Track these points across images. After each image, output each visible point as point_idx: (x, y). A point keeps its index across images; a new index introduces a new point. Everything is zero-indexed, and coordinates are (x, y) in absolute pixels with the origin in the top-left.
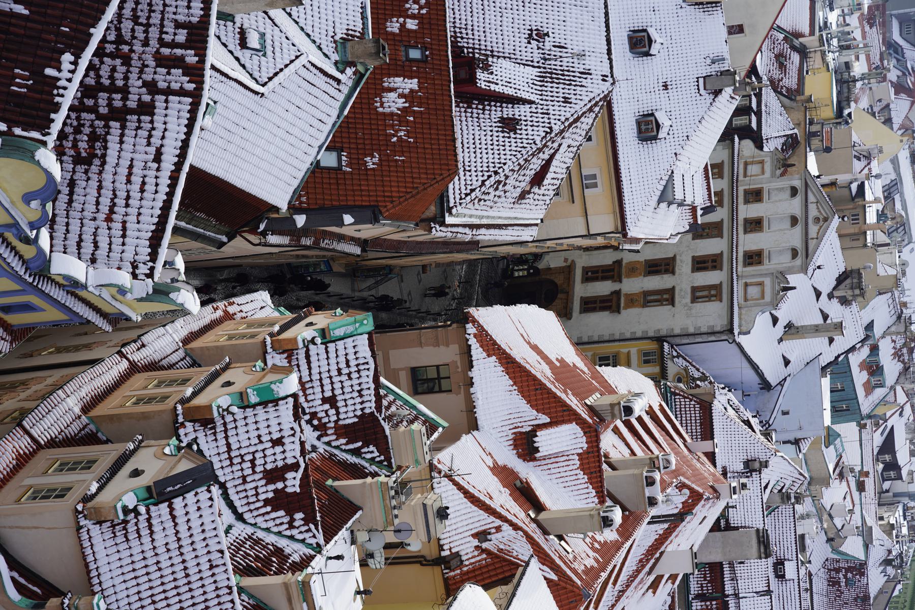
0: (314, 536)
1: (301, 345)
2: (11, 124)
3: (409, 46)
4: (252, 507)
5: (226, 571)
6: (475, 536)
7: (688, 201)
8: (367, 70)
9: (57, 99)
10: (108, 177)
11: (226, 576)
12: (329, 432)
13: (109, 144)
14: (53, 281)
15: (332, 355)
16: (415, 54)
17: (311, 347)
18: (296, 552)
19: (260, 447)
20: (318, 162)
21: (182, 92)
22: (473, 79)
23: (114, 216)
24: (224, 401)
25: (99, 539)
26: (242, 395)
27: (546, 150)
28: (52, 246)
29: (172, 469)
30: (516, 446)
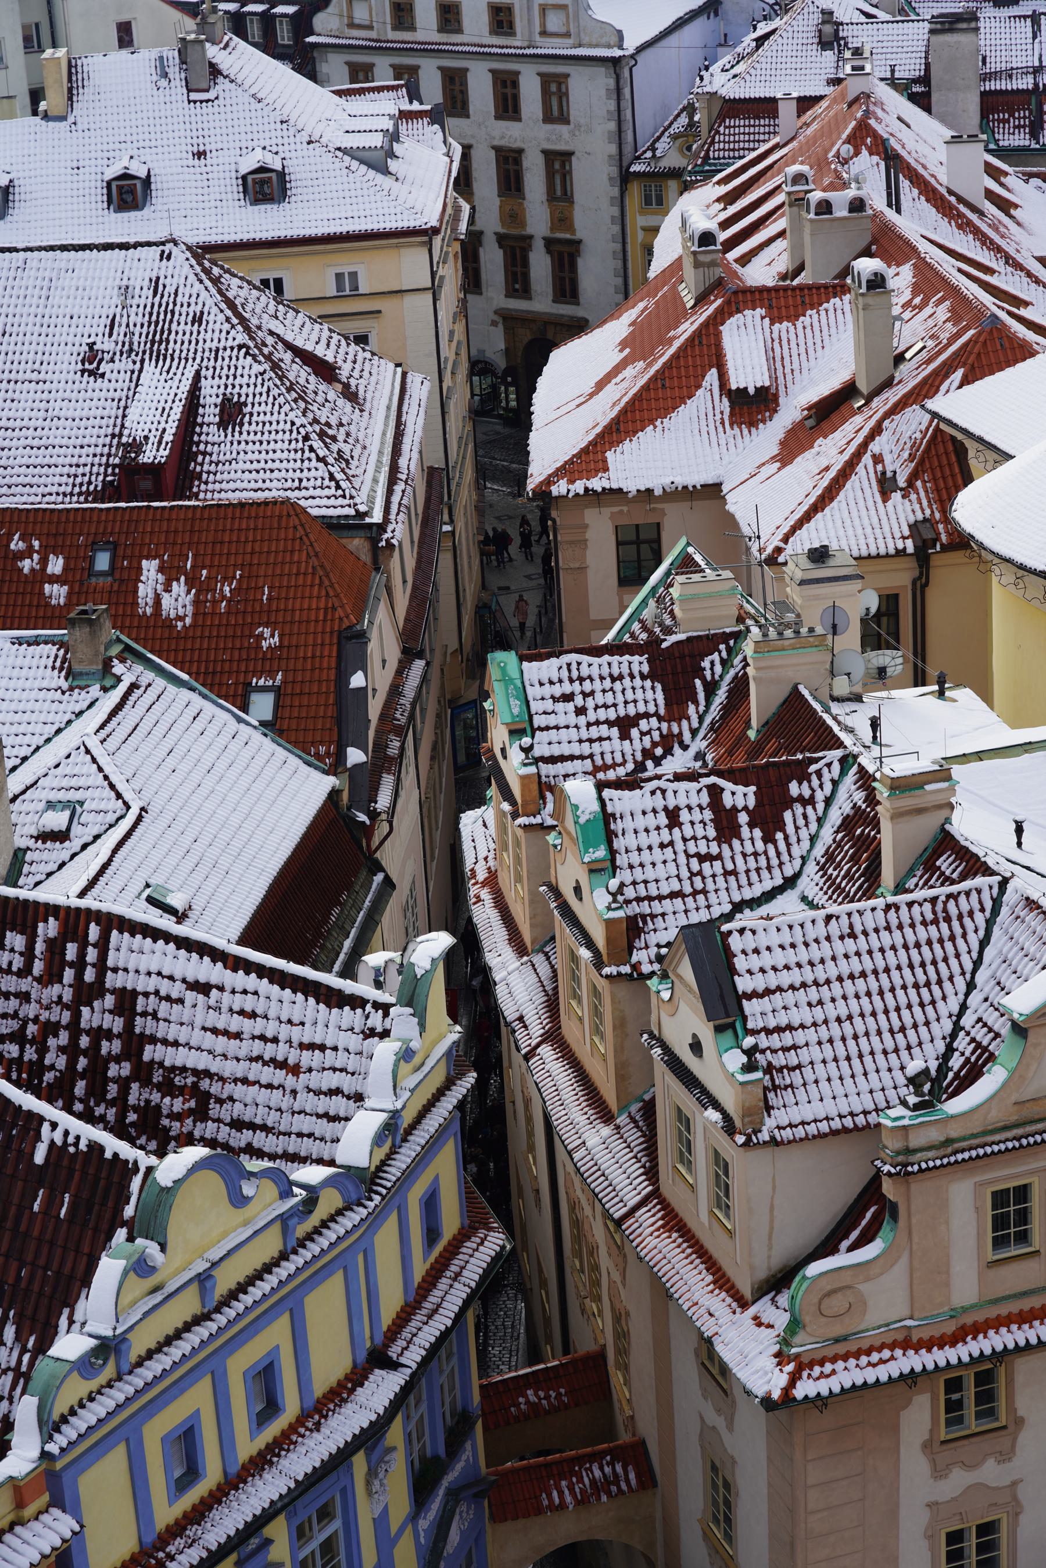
0: (829, 765)
1: (532, 770)
2: (116, 1221)
3: (90, 571)
4: (775, 862)
5: (860, 913)
6: (885, 496)
7: (389, 125)
8: (119, 640)
9: (83, 1146)
10: (229, 1068)
11: (868, 913)
12: (675, 730)
13: (178, 1063)
14: (383, 1163)
15: (551, 720)
16: (103, 561)
17: (537, 752)
18: (849, 796)
19: (679, 846)
20: (263, 724)
21: (103, 945)
22: (154, 469)
23: (291, 1062)
24: (602, 899)
25: (793, 1111)
26: (594, 870)
27: (277, 356)
28: (320, 1161)
29: (691, 991)
30: (752, 424)
